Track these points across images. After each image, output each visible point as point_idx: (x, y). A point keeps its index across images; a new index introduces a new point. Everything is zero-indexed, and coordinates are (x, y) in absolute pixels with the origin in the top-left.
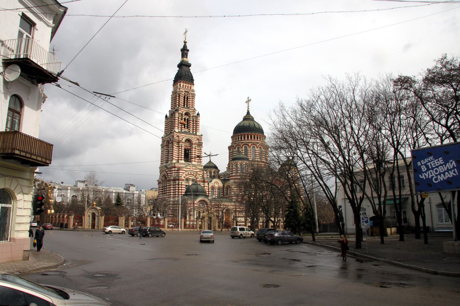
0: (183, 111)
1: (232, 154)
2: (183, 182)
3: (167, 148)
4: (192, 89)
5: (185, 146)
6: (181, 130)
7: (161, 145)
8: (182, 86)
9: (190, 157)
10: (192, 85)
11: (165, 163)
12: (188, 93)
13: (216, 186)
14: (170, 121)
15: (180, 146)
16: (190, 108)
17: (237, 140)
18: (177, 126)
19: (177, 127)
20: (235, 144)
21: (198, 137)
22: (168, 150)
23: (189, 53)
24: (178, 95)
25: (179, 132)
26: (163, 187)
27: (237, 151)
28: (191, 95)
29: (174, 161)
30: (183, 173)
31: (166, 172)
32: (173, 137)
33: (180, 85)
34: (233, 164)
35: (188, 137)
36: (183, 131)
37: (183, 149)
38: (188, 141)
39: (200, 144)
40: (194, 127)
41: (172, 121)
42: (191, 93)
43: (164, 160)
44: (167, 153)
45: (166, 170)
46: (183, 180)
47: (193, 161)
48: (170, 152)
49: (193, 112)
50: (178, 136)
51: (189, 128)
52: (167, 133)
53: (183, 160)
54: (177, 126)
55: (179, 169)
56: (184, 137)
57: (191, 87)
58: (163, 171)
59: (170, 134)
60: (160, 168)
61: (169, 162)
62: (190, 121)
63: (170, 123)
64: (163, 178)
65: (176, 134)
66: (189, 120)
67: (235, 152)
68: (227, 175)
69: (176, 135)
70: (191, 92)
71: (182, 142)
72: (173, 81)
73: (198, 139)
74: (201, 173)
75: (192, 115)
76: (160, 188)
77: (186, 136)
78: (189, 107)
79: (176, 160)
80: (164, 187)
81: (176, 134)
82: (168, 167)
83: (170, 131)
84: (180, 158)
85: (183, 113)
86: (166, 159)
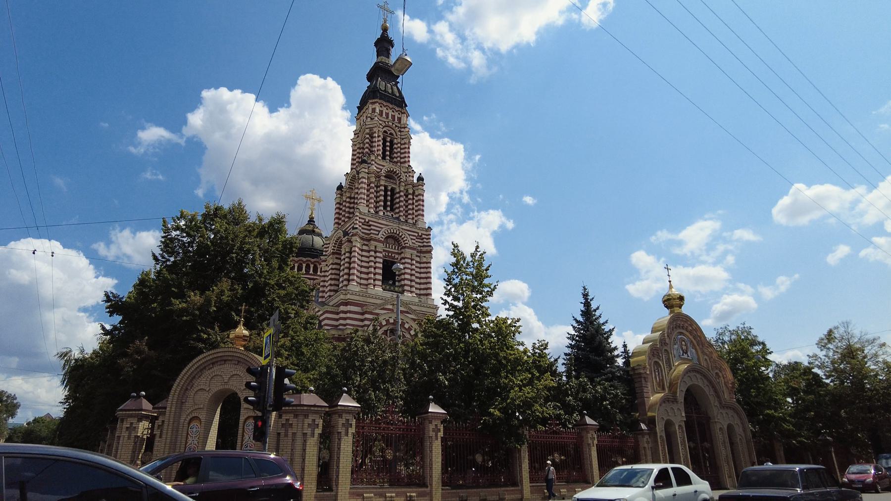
5: (384, 251)
6: (377, 212)
8: (377, 111)
10: (402, 113)
14: (348, 195)
21: (420, 232)
22: (339, 264)
33: (374, 110)
35: (394, 227)
36: (381, 213)
38: (393, 238)
39: (424, 249)
41: (353, 196)
51: (397, 211)
57: (400, 119)
62: (399, 193)
63: (348, 200)
66: (398, 191)
73: (420, 237)
77: (387, 225)
85: (381, 171)
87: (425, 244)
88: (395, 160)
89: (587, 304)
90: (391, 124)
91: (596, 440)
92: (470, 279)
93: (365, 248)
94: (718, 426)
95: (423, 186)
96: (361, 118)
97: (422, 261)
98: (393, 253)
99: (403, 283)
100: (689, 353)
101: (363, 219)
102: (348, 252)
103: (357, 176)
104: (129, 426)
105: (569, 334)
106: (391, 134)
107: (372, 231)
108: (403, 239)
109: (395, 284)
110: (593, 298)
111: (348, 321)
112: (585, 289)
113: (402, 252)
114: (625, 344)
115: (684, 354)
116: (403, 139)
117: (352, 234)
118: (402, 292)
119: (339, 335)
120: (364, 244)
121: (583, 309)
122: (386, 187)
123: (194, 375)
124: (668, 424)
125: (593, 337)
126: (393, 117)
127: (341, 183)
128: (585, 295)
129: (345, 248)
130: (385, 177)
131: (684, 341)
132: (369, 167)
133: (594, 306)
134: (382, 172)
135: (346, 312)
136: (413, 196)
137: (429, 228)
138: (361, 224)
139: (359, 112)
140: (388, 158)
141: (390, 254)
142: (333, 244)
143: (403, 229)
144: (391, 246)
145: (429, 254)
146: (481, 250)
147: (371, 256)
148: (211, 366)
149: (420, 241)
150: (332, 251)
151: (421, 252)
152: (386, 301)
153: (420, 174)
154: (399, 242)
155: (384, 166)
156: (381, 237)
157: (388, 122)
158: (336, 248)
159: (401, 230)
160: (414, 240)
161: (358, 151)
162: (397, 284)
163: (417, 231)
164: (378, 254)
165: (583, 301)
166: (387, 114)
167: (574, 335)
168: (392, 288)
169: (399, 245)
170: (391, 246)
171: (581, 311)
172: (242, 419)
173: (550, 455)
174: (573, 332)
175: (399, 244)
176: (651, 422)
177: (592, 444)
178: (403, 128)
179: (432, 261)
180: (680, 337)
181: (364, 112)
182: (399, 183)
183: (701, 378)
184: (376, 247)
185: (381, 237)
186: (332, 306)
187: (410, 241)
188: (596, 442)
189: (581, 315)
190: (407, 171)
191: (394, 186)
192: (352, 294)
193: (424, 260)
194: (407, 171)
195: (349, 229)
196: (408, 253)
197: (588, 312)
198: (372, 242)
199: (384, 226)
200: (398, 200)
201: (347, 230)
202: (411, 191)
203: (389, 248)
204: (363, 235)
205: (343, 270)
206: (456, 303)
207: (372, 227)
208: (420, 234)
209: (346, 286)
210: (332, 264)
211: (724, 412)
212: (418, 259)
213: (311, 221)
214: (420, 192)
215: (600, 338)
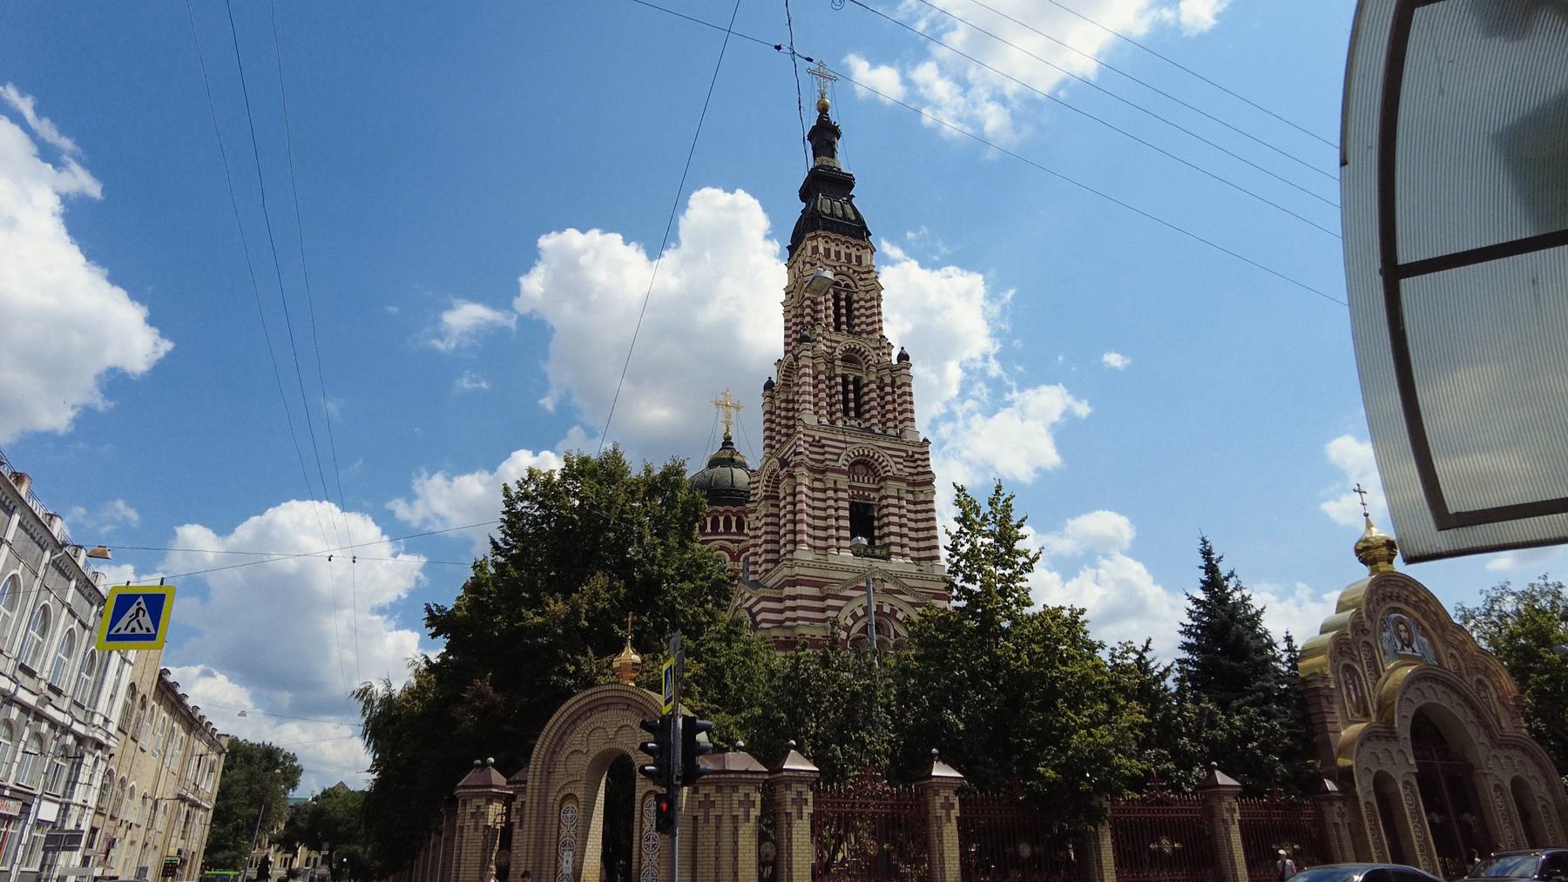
3: (775, 510)
4: (864, 264)
6: (832, 423)
8: (821, 250)
9: (881, 538)
10: (864, 248)
14: (783, 396)
16: (864, 335)
22: (777, 515)
23: (839, 144)
33: (815, 250)
36: (840, 424)
38: (864, 464)
39: (920, 478)
41: (790, 397)
47: (897, 554)
51: (867, 416)
57: (859, 259)
62: (867, 385)
63: (783, 405)
66: (866, 381)
70: (863, 276)
78: (863, 331)
85: (835, 351)
87: (920, 469)
88: (857, 329)
89: (1211, 568)
90: (846, 269)
91: (1238, 812)
92: (990, 544)
93: (817, 485)
94: (1491, 782)
95: (908, 369)
96: (795, 265)
97: (917, 500)
98: (864, 489)
99: (887, 540)
100: (1415, 646)
101: (809, 436)
102: (790, 495)
103: (795, 364)
104: (474, 811)
105: (1183, 625)
106: (847, 286)
107: (827, 456)
108: (880, 464)
109: (874, 544)
110: (1221, 557)
111: (800, 613)
112: (1205, 542)
113: (882, 488)
114: (1289, 635)
115: (1405, 648)
116: (867, 292)
117: (793, 463)
118: (887, 557)
119: (786, 637)
120: (816, 480)
121: (1204, 578)
122: (844, 377)
123: (563, 728)
124: (1382, 783)
125: (1225, 628)
126: (848, 256)
127: (770, 378)
128: (1207, 554)
129: (784, 488)
130: (842, 360)
131: (1401, 623)
132: (814, 347)
133: (1224, 569)
135: (794, 598)
136: (893, 388)
137: (925, 440)
138: (807, 446)
139: (791, 255)
140: (844, 327)
141: (861, 493)
142: (765, 483)
143: (879, 447)
144: (861, 478)
146: (1006, 493)
147: (829, 498)
148: (589, 714)
149: (912, 465)
150: (764, 494)
151: (914, 484)
152: (862, 575)
154: (876, 470)
155: (839, 342)
156: (844, 465)
158: (770, 489)
159: (877, 449)
160: (901, 463)
161: (794, 320)
162: (877, 542)
163: (904, 447)
164: (841, 495)
165: (1203, 563)
166: (838, 254)
167: (1192, 625)
168: (869, 551)
169: (876, 474)
170: (861, 478)
171: (1202, 581)
172: (639, 796)
173: (1153, 842)
174: (1190, 622)
175: (875, 473)
176: (1345, 777)
177: (1230, 820)
179: (935, 498)
180: (1394, 615)
181: (799, 255)
182: (867, 368)
183: (1444, 692)
184: (835, 482)
185: (844, 465)
186: (771, 588)
187: (893, 464)
188: (1237, 816)
189: (1202, 588)
191: (857, 374)
192: (802, 565)
193: (922, 497)
195: (788, 454)
196: (892, 488)
197: (1213, 581)
198: (829, 474)
199: (848, 444)
200: (866, 398)
201: (785, 457)
202: (888, 380)
203: (858, 481)
204: (813, 463)
205: (785, 525)
206: (969, 586)
207: (827, 449)
208: (910, 454)
209: (792, 552)
210: (766, 516)
211: (1497, 752)
212: (910, 497)
213: (727, 443)
214: (905, 379)
215: (1237, 628)
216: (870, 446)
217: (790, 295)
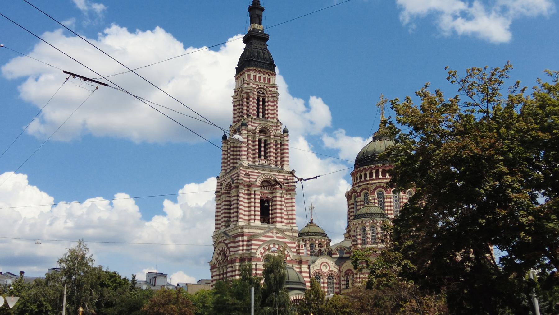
0: (255, 125)
1: (353, 208)
2: (258, 263)
3: (228, 199)
4: (271, 83)
7: (216, 192)
8: (252, 77)
10: (272, 74)
11: (223, 227)
12: (264, 92)
13: (325, 270)
14: (232, 145)
15: (253, 192)
17: (363, 179)
18: (244, 155)
19: (246, 157)
20: (358, 186)
22: (229, 201)
24: (245, 95)
25: (250, 167)
26: (220, 275)
27: (363, 201)
28: (270, 95)
29: (241, 223)
30: (260, 246)
31: (226, 244)
32: (238, 176)
33: (249, 76)
34: (357, 225)
37: (258, 199)
39: (290, 188)
40: (278, 156)
41: (235, 145)
42: (270, 91)
43: (222, 222)
44: (226, 207)
45: (226, 240)
46: (259, 260)
47: (279, 222)
48: (234, 204)
49: (276, 128)
50: (247, 175)
52: (226, 168)
53: (258, 220)
54: (244, 155)
55: (252, 238)
56: (258, 176)
57: (269, 80)
58: (221, 242)
59: (231, 170)
60: (214, 237)
61: (232, 226)
62: (270, 144)
63: (232, 149)
64: (221, 257)
65: (243, 171)
66: (269, 143)
67: (359, 204)
68: (345, 249)
69: (244, 173)
70: (270, 89)
71: (256, 186)
72: (236, 68)
74: (293, 245)
75: (273, 133)
76: (215, 278)
78: (268, 118)
79: (244, 220)
80: (223, 274)
81: (243, 171)
82: (230, 234)
83: (231, 165)
84: (252, 217)
85: (256, 129)
86: (226, 219)
95: (287, 137)
101: (244, 171)
102: (236, 196)
106: (263, 93)
113: (274, 192)
129: (233, 191)
134: (257, 130)
142: (225, 186)
145: (294, 192)
153: (286, 127)
156: (259, 183)
157: (261, 85)
158: (227, 189)
178: (271, 87)
185: (259, 183)
190: (276, 125)
194: (276, 125)
216: (270, 175)
217: (236, 93)
